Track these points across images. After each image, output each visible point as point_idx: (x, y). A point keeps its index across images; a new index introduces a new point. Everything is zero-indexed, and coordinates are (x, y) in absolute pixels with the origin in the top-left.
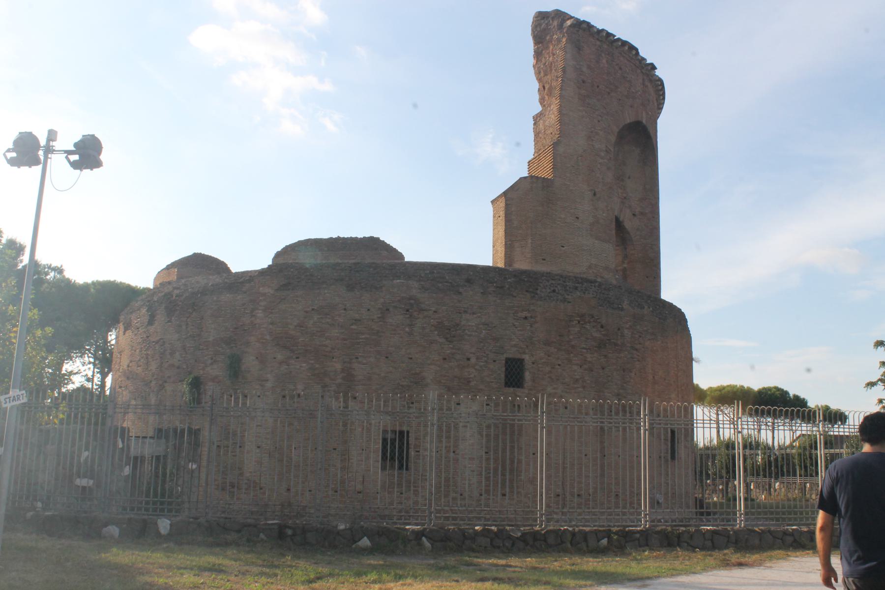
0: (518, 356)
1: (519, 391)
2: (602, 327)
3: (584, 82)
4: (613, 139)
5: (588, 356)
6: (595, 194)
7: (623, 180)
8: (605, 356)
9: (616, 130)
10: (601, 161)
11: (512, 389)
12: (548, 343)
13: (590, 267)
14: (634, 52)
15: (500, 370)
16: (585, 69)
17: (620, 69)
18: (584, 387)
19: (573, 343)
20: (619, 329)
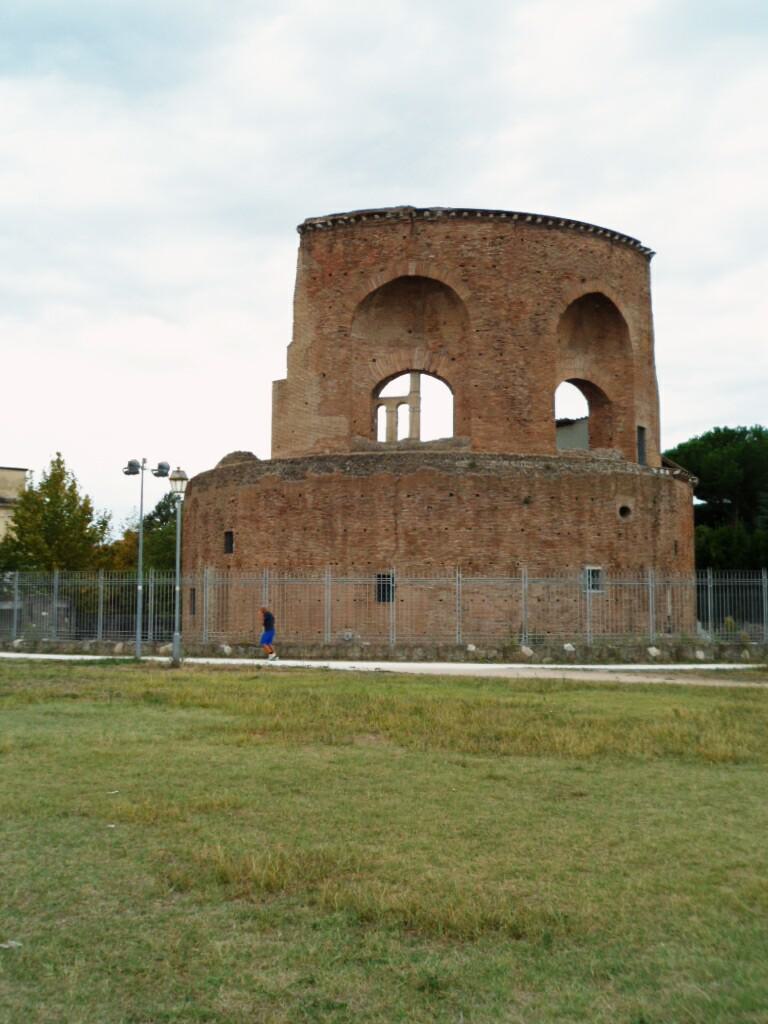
0: (230, 530)
1: (231, 556)
2: (283, 496)
3: (315, 279)
4: (348, 316)
5: (272, 522)
6: (324, 375)
7: (438, 329)
8: (285, 520)
9: (352, 305)
10: (332, 343)
11: (225, 556)
12: (244, 518)
13: (318, 442)
14: (377, 216)
15: (221, 540)
16: (316, 266)
17: (365, 240)
18: (269, 547)
19: (261, 514)
20: (300, 495)
